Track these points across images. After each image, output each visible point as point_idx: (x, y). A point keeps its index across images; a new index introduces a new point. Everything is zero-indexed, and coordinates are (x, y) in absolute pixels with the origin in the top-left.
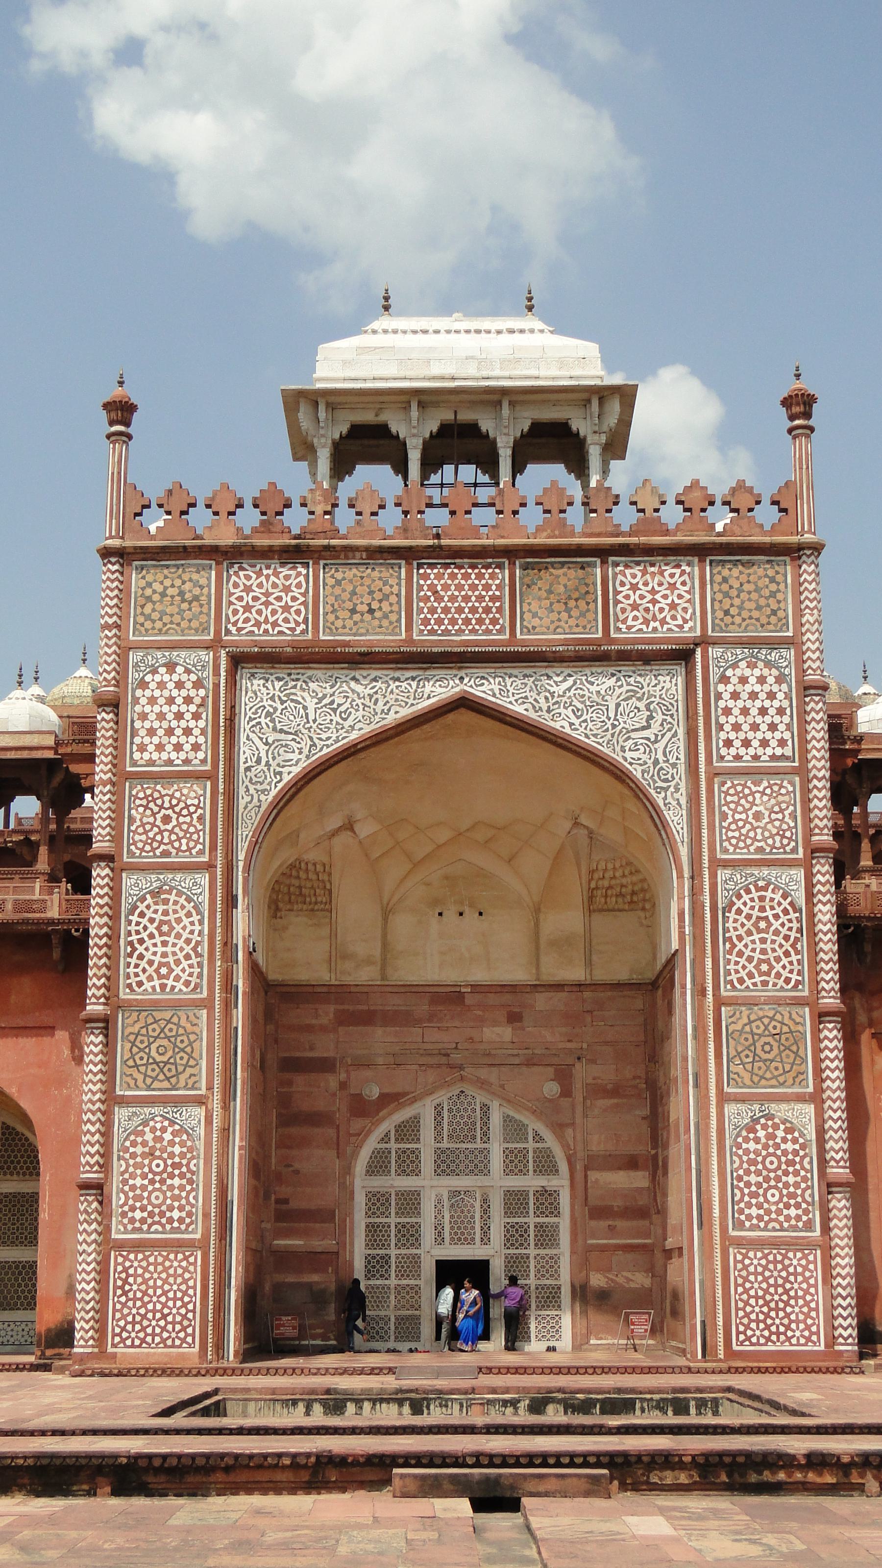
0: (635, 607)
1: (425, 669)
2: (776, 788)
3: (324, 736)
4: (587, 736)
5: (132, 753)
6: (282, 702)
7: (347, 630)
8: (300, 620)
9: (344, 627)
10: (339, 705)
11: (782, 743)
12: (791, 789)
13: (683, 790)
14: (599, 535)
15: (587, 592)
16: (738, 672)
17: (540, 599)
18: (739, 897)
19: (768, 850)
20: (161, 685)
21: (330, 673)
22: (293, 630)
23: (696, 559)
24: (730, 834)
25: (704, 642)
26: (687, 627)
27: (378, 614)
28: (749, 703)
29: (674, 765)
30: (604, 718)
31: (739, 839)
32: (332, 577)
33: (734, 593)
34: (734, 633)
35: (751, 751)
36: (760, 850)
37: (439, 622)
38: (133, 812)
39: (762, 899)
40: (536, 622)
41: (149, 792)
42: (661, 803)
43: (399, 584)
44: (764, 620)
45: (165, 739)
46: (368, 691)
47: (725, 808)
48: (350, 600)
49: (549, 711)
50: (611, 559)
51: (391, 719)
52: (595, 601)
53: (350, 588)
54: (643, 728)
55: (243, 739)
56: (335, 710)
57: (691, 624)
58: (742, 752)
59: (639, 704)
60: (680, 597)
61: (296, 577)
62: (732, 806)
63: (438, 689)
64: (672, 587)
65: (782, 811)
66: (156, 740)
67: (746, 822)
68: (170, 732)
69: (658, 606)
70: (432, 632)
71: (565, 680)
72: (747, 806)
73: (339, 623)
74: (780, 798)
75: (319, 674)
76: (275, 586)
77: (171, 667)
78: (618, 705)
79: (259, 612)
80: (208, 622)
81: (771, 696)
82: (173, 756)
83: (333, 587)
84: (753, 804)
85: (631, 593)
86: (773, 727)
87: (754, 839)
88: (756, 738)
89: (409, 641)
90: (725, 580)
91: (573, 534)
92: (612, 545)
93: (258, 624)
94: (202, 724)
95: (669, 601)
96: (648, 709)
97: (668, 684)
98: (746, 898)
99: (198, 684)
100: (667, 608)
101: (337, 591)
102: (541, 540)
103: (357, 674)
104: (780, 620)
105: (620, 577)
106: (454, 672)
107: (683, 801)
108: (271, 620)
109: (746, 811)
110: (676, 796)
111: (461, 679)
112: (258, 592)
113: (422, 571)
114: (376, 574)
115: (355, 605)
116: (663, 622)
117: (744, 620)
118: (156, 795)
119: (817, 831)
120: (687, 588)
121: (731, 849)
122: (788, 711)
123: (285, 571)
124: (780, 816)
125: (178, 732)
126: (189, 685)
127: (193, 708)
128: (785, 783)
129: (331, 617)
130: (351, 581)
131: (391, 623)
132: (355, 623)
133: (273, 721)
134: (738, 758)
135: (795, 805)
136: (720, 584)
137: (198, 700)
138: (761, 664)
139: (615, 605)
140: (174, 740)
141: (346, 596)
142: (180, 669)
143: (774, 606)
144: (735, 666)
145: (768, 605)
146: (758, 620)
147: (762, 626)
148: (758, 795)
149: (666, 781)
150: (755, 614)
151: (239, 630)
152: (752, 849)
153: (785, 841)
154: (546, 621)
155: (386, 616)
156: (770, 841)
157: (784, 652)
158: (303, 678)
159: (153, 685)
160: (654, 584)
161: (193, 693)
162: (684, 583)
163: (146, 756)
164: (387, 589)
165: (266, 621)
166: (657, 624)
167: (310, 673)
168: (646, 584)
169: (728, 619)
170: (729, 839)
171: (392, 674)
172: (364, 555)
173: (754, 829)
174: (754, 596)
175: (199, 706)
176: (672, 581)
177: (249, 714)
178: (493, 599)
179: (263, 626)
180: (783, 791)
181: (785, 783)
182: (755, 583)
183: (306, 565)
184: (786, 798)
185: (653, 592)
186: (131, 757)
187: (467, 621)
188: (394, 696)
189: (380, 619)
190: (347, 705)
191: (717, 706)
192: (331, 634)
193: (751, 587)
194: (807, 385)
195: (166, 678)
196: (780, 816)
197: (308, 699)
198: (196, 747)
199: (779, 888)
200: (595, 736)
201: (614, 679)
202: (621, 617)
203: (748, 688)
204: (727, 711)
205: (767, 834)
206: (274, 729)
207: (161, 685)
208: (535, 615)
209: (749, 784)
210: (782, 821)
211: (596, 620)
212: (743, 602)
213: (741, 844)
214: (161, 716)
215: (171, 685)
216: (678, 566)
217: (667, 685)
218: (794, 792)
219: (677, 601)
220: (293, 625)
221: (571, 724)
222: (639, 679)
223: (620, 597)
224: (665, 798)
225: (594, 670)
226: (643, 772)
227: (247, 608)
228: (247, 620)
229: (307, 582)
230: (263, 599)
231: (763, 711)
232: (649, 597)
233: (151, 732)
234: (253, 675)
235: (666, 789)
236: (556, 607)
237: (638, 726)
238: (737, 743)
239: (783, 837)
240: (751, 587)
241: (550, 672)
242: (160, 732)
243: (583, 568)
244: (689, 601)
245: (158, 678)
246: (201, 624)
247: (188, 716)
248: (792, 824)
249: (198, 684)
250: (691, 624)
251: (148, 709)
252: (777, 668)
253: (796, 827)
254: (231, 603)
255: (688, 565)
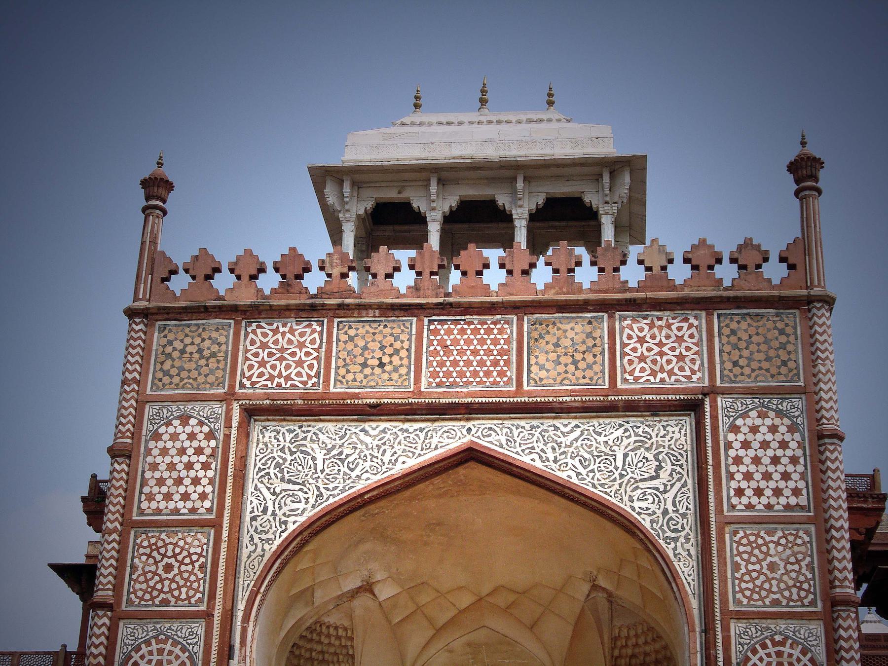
0: (642, 359)
1: (434, 421)
2: (791, 538)
3: (331, 486)
4: (594, 486)
5: (140, 502)
6: (292, 453)
7: (357, 384)
8: (313, 374)
9: (355, 380)
10: (348, 456)
11: (796, 492)
12: (807, 539)
13: (692, 541)
14: (606, 291)
15: (595, 345)
16: (749, 422)
17: (547, 352)
18: (755, 652)
19: (784, 602)
20: (174, 437)
21: (340, 425)
22: (305, 383)
23: (704, 314)
24: (744, 585)
25: (712, 391)
26: (695, 378)
27: (388, 368)
28: (760, 453)
29: (684, 516)
30: (611, 468)
31: (753, 591)
32: (346, 333)
33: (743, 345)
34: (743, 383)
35: (764, 500)
36: (776, 602)
37: (448, 374)
38: (136, 560)
39: (779, 654)
40: (543, 374)
41: (153, 541)
42: (671, 553)
43: (409, 340)
44: (774, 371)
45: (174, 489)
46: (376, 442)
47: (738, 559)
48: (362, 355)
49: (555, 461)
50: (618, 314)
51: (399, 469)
52: (602, 353)
53: (361, 343)
54: (652, 478)
55: (250, 488)
56: (343, 461)
57: (699, 374)
58: (754, 500)
59: (647, 455)
60: (688, 349)
61: (310, 333)
62: (745, 556)
63: (448, 438)
64: (680, 339)
65: (798, 562)
66: (164, 490)
67: (760, 573)
68: (179, 481)
69: (665, 358)
70: (441, 384)
71: (572, 431)
72: (761, 556)
73: (350, 377)
74: (796, 549)
75: (330, 426)
76: (290, 342)
77: (185, 419)
78: (626, 455)
79: (274, 367)
80: (224, 377)
81: (784, 445)
82: (180, 504)
83: (346, 342)
84: (767, 554)
85: (638, 345)
86: (786, 476)
87: (770, 591)
88: (768, 488)
89: (418, 393)
90: (733, 332)
91: (580, 290)
92: (618, 300)
93: (271, 378)
94: (210, 473)
95: (677, 353)
96: (657, 459)
97: (677, 432)
98: (762, 653)
99: (210, 436)
100: (675, 360)
101: (350, 346)
102: (550, 296)
103: (367, 426)
104: (790, 370)
105: (627, 331)
106: (462, 423)
107: (693, 552)
108: (284, 374)
109: (759, 562)
110: (687, 546)
111: (469, 430)
112: (273, 348)
113: (432, 327)
114: (388, 330)
115: (367, 359)
116: (671, 373)
117: (753, 370)
118: (160, 543)
119: (837, 583)
120: (694, 341)
121: (745, 601)
122: (802, 460)
123: (300, 328)
124: (796, 567)
125: (187, 481)
126: (201, 436)
127: (203, 459)
128: (801, 534)
129: (342, 371)
130: (363, 338)
131: (401, 376)
132: (366, 377)
133: (281, 471)
134: (750, 507)
135: (811, 556)
136: (728, 336)
137: (208, 451)
138: (772, 414)
139: (622, 358)
140: (182, 489)
141: (358, 351)
142: (193, 422)
143: (784, 357)
144: (745, 415)
145: (778, 356)
146: (767, 370)
147: (772, 376)
148: (772, 546)
149: (676, 531)
150: (765, 365)
151: (253, 384)
152: (767, 601)
153: (803, 594)
154: (553, 374)
155: (396, 370)
156: (786, 593)
157: (796, 403)
158: (313, 430)
159: (166, 437)
160: (661, 336)
161: (204, 444)
162: (691, 336)
163: (154, 505)
164: (397, 345)
165: (280, 375)
166: (665, 375)
167: (321, 425)
168: (653, 337)
169: (737, 370)
170: (742, 591)
171: (400, 425)
172: (377, 313)
173: (769, 580)
174: (763, 347)
175: (209, 456)
176: (680, 334)
177: (259, 465)
178: (501, 352)
179: (277, 380)
180: (799, 541)
181: (801, 534)
182: (764, 336)
183: (321, 323)
184: (803, 549)
185: (660, 344)
186: (139, 507)
187: (475, 374)
188: (403, 447)
189: (390, 373)
190: (355, 456)
191: (727, 456)
192: (342, 387)
193: (760, 339)
194: (813, 150)
195: (180, 429)
196: (796, 567)
197: (318, 450)
198: (203, 496)
199: (798, 643)
200: (602, 485)
201: (622, 430)
202: (629, 369)
203: (759, 437)
204: (738, 461)
205: (782, 586)
206: (283, 480)
207: (174, 437)
208: (542, 367)
209: (762, 533)
210: (799, 572)
211: (603, 372)
212: (752, 354)
213: (756, 596)
214: (171, 467)
215: (183, 437)
216: (686, 320)
217: (677, 435)
218: (810, 542)
219: (684, 353)
220: (305, 379)
221: (578, 474)
222: (647, 429)
223: (627, 350)
224: (675, 549)
225: (601, 421)
226: (652, 522)
227: (262, 364)
228: (261, 375)
229: (321, 340)
230: (279, 355)
231: (775, 460)
232: (657, 349)
233: (161, 482)
234: (265, 428)
235: (676, 540)
236: (563, 360)
237: (646, 476)
238: (749, 492)
239: (800, 589)
240: (760, 339)
241: (557, 423)
242: (170, 482)
243: (590, 323)
244: (696, 353)
245: (171, 430)
246: (217, 378)
247: (198, 466)
248: (810, 576)
249: (210, 436)
250: (699, 374)
251: (159, 459)
252: (789, 418)
253: (813, 579)
254: (247, 359)
255: (696, 318)
